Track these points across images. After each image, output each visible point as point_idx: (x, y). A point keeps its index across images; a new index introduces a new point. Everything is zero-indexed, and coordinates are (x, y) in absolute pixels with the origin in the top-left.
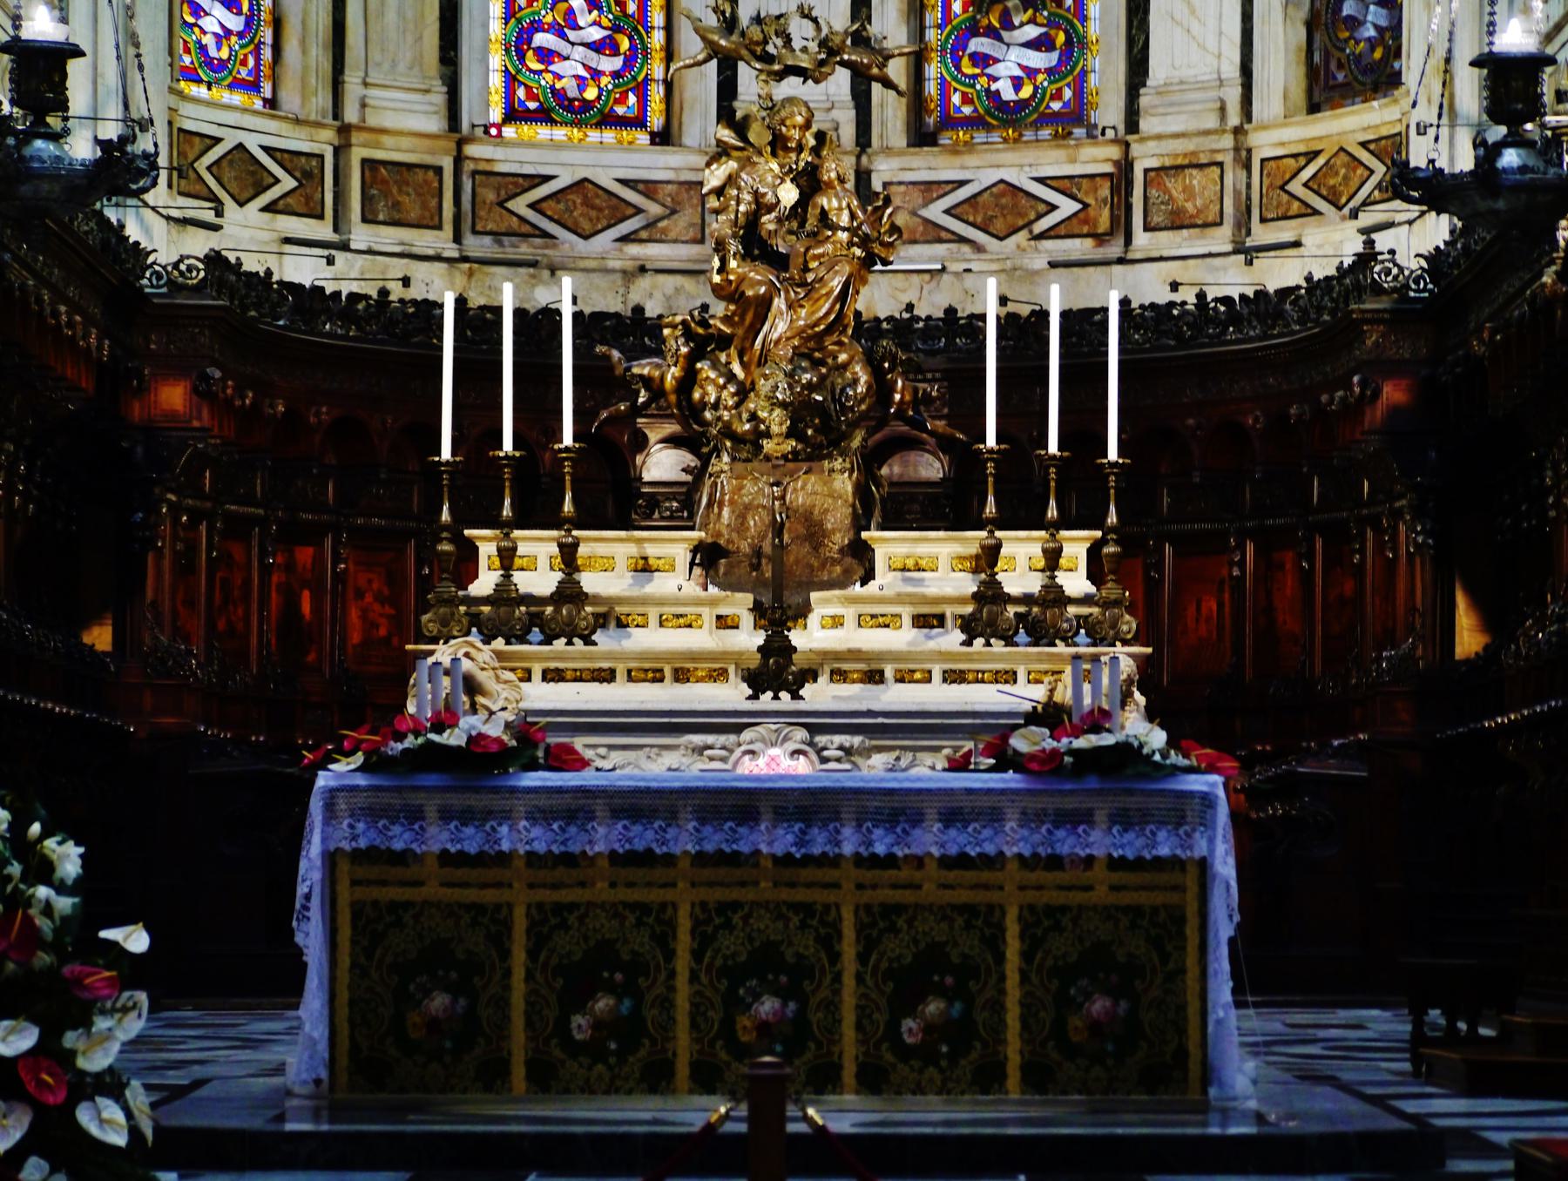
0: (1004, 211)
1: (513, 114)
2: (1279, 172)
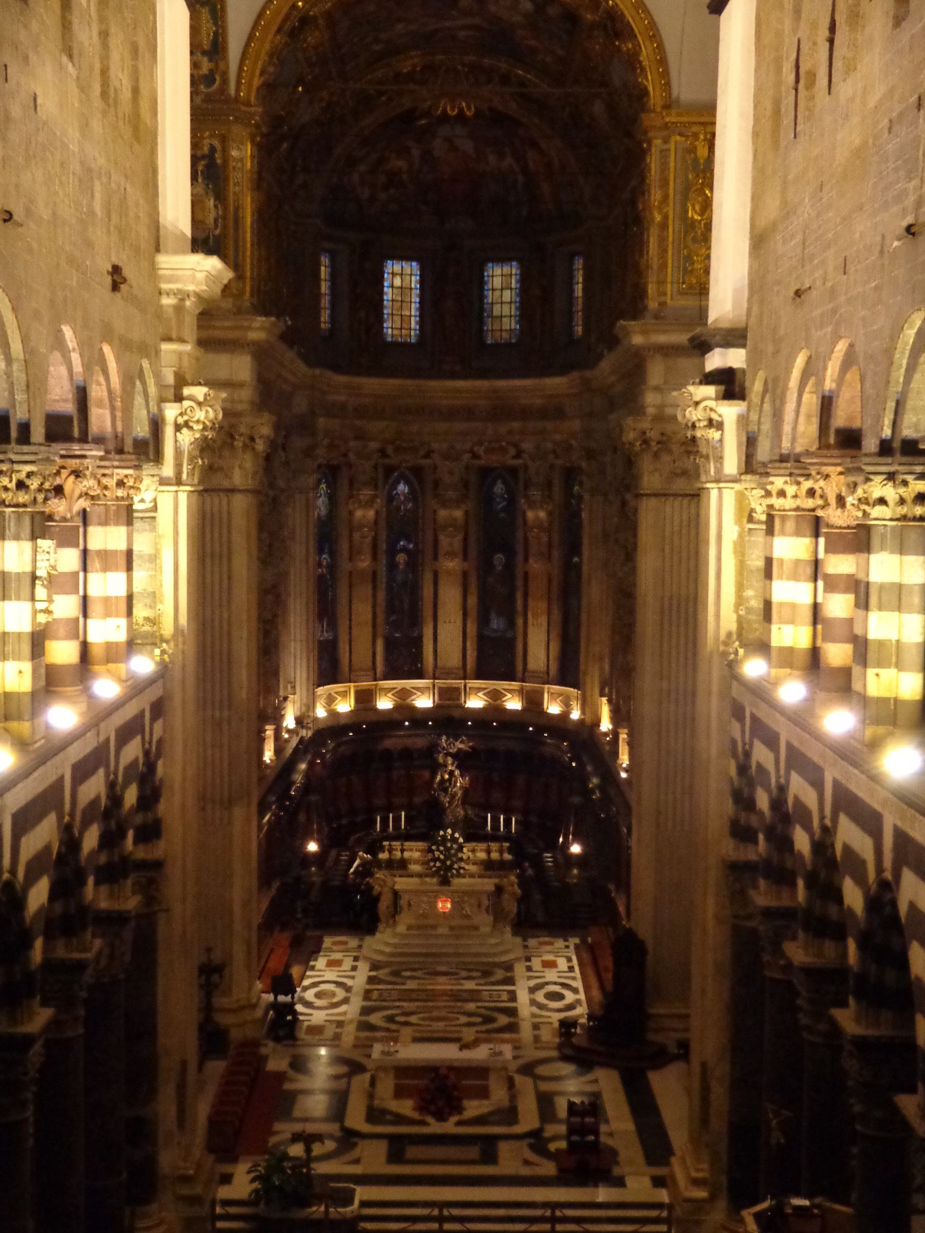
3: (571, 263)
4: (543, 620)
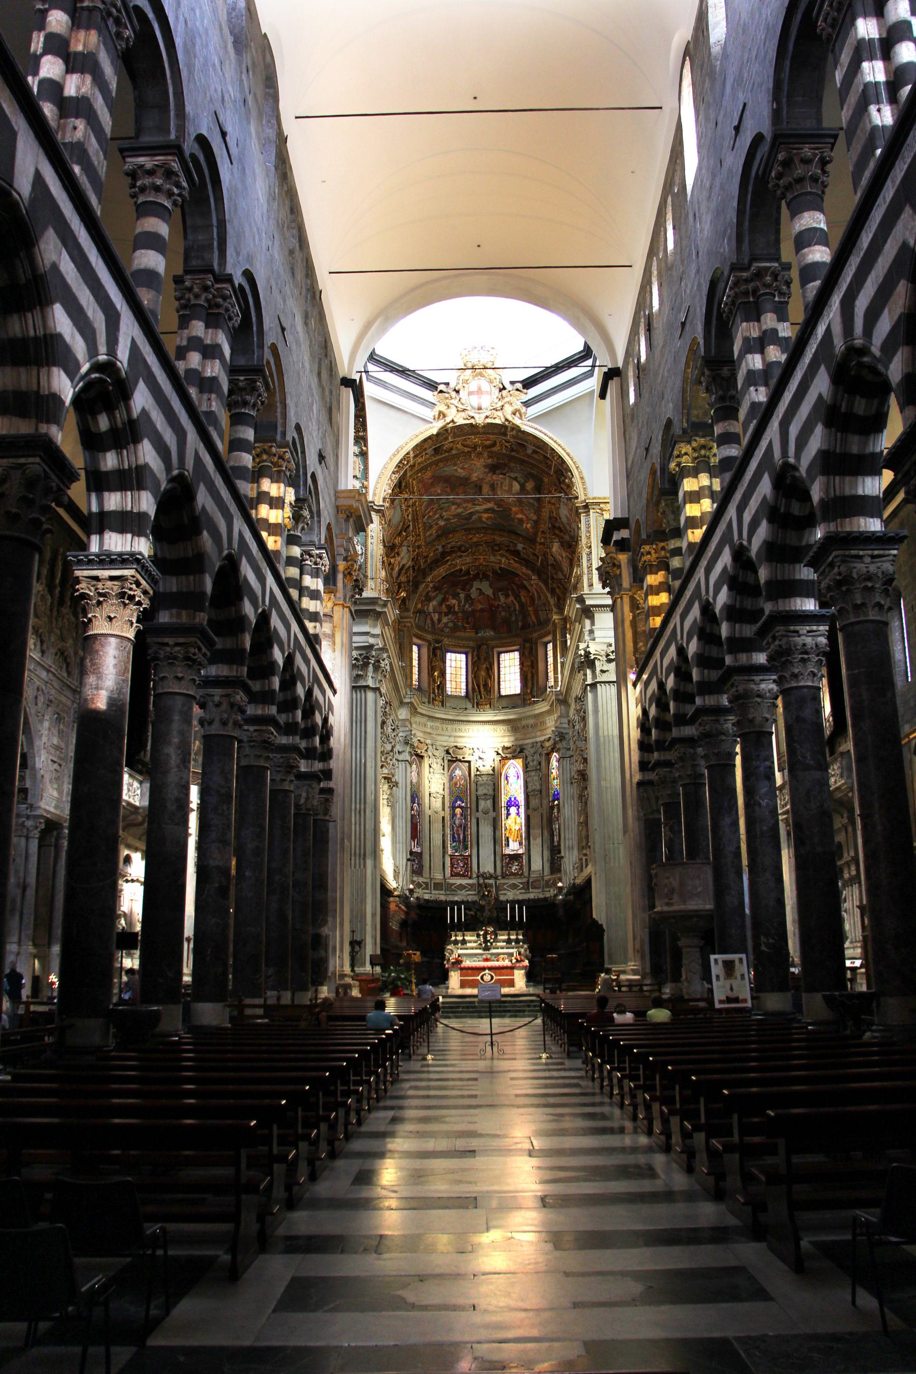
0: (514, 886)
1: (452, 875)
2: (547, 882)
3: (546, 648)
4: (539, 840)
